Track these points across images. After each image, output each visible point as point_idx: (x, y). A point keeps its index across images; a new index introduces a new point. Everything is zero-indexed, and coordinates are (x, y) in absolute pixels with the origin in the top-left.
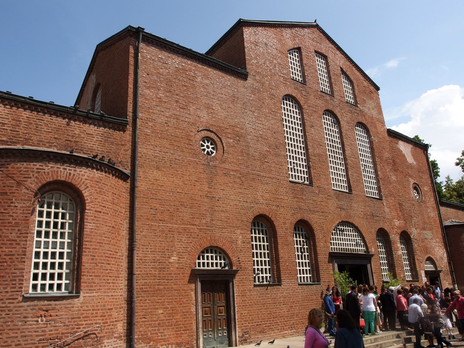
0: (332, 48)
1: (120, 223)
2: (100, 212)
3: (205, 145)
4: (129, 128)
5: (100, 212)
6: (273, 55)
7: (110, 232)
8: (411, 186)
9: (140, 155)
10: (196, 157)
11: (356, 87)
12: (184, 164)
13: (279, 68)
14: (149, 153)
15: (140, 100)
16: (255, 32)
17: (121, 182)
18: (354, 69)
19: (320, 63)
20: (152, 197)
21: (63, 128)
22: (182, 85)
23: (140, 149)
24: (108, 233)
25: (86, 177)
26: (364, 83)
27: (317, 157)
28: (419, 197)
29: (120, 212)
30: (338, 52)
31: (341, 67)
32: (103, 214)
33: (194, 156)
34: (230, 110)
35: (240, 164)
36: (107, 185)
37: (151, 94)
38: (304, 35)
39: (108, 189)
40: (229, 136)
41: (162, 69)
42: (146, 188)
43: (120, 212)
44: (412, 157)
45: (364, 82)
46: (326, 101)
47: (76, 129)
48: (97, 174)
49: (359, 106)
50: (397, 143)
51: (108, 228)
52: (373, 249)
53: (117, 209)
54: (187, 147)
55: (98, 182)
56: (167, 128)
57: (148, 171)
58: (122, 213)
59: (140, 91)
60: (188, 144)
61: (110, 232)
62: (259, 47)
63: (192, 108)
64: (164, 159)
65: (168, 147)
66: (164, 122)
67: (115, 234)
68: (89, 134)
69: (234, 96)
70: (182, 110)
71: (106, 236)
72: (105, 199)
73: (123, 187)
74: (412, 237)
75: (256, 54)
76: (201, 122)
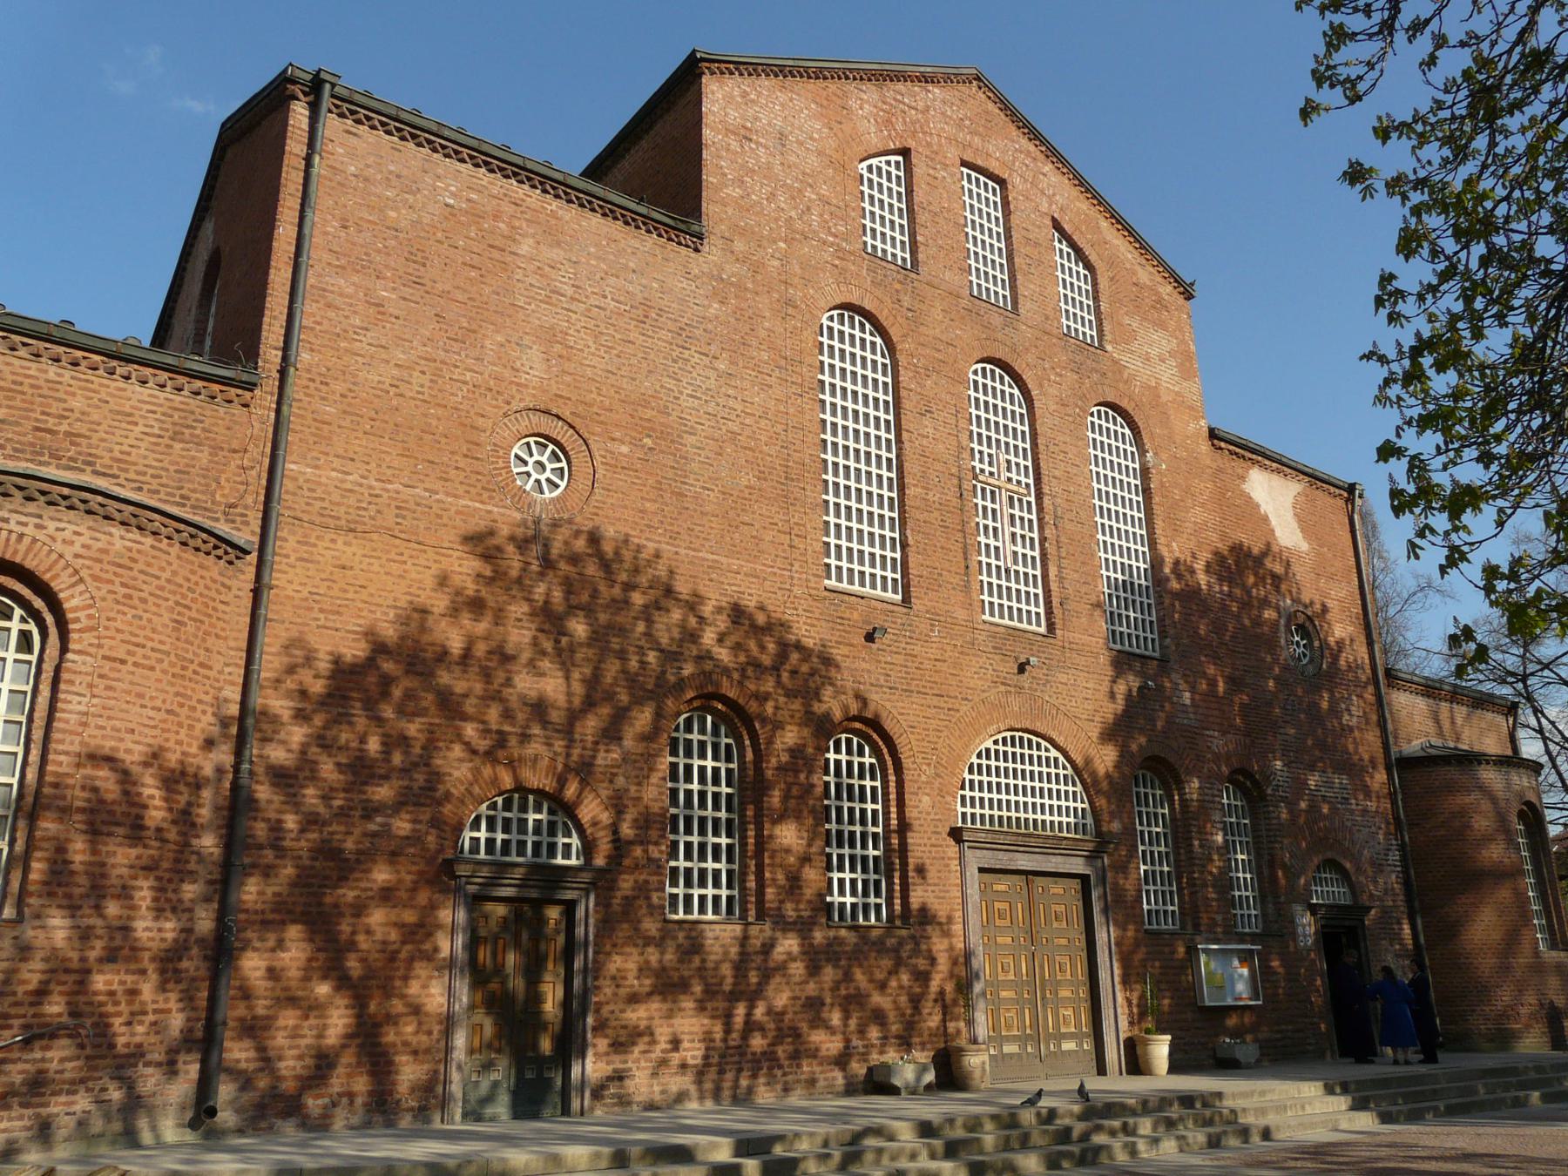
0: (1028, 153)
1: (200, 701)
2: (123, 662)
4: (264, 398)
5: (123, 662)
6: (804, 174)
7: (154, 727)
10: (491, 498)
11: (1103, 283)
12: (445, 520)
13: (821, 215)
14: (323, 480)
15: (309, 310)
16: (744, 94)
17: (214, 568)
18: (1104, 224)
19: (980, 200)
20: (321, 623)
21: (30, 391)
22: (464, 264)
23: (292, 466)
24: (146, 731)
25: (77, 548)
26: (1134, 273)
27: (936, 514)
28: (1311, 661)
29: (201, 665)
30: (1048, 168)
31: (1054, 219)
32: (132, 669)
33: (486, 495)
34: (630, 349)
35: (648, 526)
36: (158, 578)
37: (351, 290)
38: (927, 109)
39: (161, 588)
40: (618, 435)
41: (396, 209)
42: (305, 594)
43: (201, 665)
44: (1295, 525)
45: (1138, 268)
46: (987, 327)
47: (74, 394)
48: (119, 539)
49: (1109, 348)
50: (1243, 478)
51: (152, 713)
53: (190, 656)
54: (461, 465)
55: (120, 566)
56: (395, 403)
57: (318, 538)
58: (210, 668)
59: (310, 279)
60: (466, 456)
61: (154, 727)
62: (757, 143)
63: (492, 341)
64: (378, 500)
65: (395, 464)
66: (388, 381)
67: (177, 733)
68: (118, 413)
69: (646, 304)
70: (456, 346)
71: (136, 737)
72: (144, 622)
73: (223, 585)
74: (1269, 791)
75: (742, 166)
76: (518, 384)
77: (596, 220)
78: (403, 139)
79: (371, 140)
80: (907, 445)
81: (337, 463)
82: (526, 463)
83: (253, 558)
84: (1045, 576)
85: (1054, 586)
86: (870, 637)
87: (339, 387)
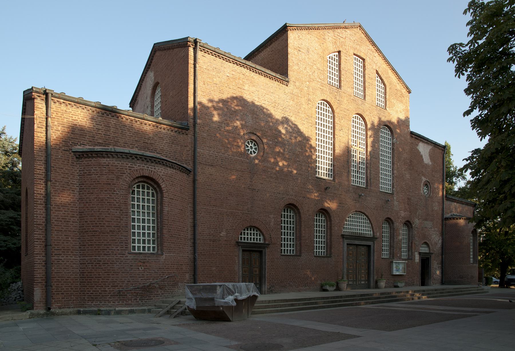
3: (249, 146)
8: (422, 184)
9: (198, 155)
17: (185, 176)
52: (378, 234)
77: (262, 78)
78: (216, 57)
79: (209, 57)
80: (336, 139)
81: (207, 148)
82: (248, 147)
83: (192, 173)
84: (367, 173)
85: (369, 175)
86: (326, 189)
87: (207, 128)
